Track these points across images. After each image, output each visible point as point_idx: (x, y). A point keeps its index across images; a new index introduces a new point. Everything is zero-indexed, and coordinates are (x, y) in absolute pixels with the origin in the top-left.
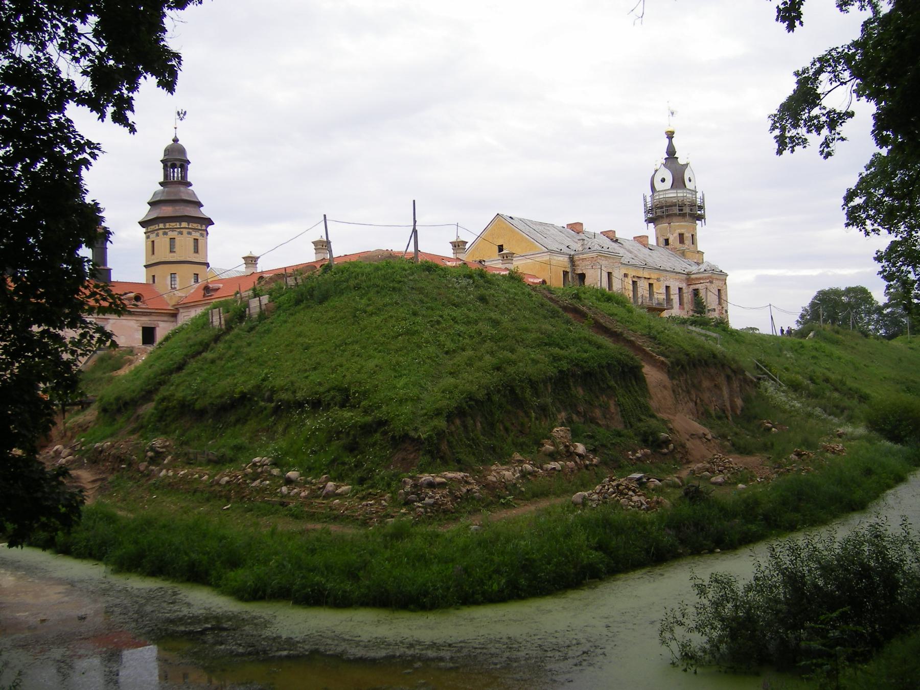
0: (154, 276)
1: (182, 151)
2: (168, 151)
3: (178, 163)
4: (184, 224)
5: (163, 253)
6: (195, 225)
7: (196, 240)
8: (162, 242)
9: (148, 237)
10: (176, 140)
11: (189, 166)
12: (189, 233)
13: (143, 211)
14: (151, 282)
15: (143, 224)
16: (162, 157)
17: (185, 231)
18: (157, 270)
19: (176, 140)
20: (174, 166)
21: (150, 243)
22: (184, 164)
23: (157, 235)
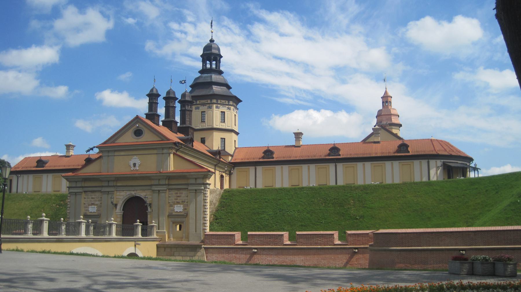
10: (212, 41)
19: (212, 41)
22: (217, 57)
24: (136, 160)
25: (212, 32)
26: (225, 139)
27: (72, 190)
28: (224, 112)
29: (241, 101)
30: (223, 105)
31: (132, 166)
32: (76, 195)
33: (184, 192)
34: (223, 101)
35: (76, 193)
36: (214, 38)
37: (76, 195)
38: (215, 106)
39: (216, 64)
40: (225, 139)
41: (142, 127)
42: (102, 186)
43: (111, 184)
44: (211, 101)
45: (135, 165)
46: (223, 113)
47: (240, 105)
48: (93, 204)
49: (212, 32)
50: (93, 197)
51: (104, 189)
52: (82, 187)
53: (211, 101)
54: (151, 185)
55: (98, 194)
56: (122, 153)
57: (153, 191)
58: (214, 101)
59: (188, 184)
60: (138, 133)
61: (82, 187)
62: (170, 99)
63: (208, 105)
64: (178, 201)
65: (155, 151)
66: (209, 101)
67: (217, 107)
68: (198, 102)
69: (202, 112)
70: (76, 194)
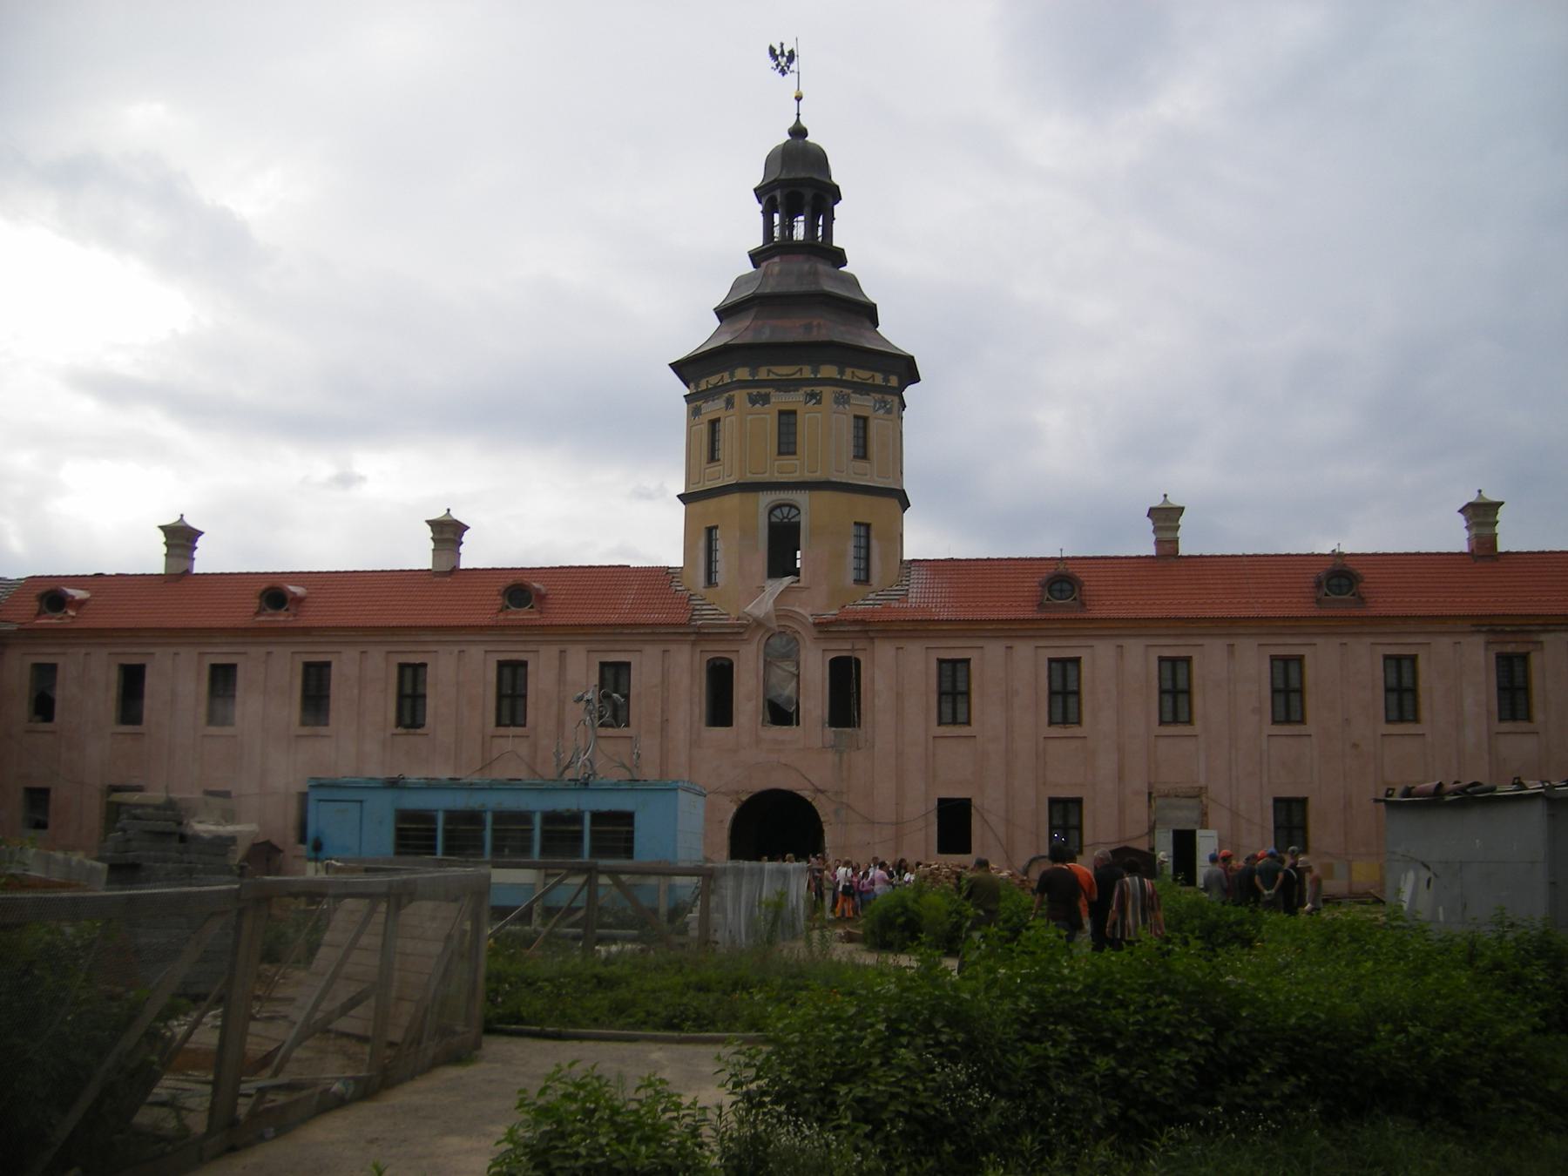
1: (818, 159)
6: (784, 371)
10: (798, 132)
19: (798, 132)
25: (799, 98)
26: (868, 526)
28: (865, 419)
29: (915, 378)
30: (863, 388)
34: (863, 375)
36: (804, 122)
38: (828, 392)
44: (815, 371)
46: (862, 423)
47: (910, 393)
49: (799, 98)
53: (815, 371)
58: (829, 371)
66: (807, 372)
67: (841, 400)
68: (763, 374)
69: (781, 413)
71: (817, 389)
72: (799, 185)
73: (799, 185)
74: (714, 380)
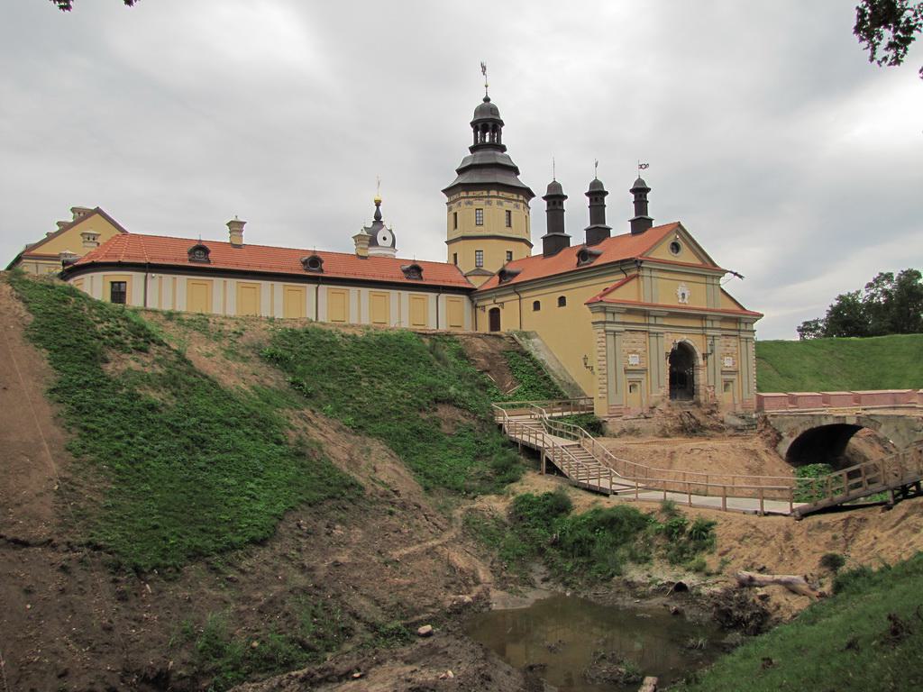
0: (455, 255)
2: (479, 111)
3: (490, 124)
4: (493, 193)
5: (468, 228)
7: (509, 212)
8: (466, 211)
9: (450, 209)
10: (487, 100)
11: (503, 129)
12: (501, 204)
13: (452, 179)
14: (452, 262)
15: (447, 191)
16: (472, 119)
17: (494, 201)
18: (460, 247)
19: (487, 100)
20: (484, 131)
21: (452, 216)
23: (459, 204)
24: (682, 288)
25: (486, 86)
27: (609, 327)
31: (681, 297)
32: (615, 335)
33: (733, 341)
35: (615, 332)
37: (615, 335)
39: (492, 137)
40: (511, 253)
41: (680, 242)
42: (649, 324)
43: (659, 321)
45: (683, 294)
48: (634, 352)
49: (486, 86)
50: (634, 340)
51: (652, 329)
52: (624, 323)
54: (703, 328)
55: (641, 336)
56: (667, 275)
57: (707, 336)
59: (739, 330)
60: (675, 247)
61: (624, 323)
62: (597, 195)
63: (514, 202)
64: (728, 351)
65: (703, 280)
70: (615, 333)
71: (518, 203)
72: (487, 123)
73: (487, 123)
74: (478, 193)
